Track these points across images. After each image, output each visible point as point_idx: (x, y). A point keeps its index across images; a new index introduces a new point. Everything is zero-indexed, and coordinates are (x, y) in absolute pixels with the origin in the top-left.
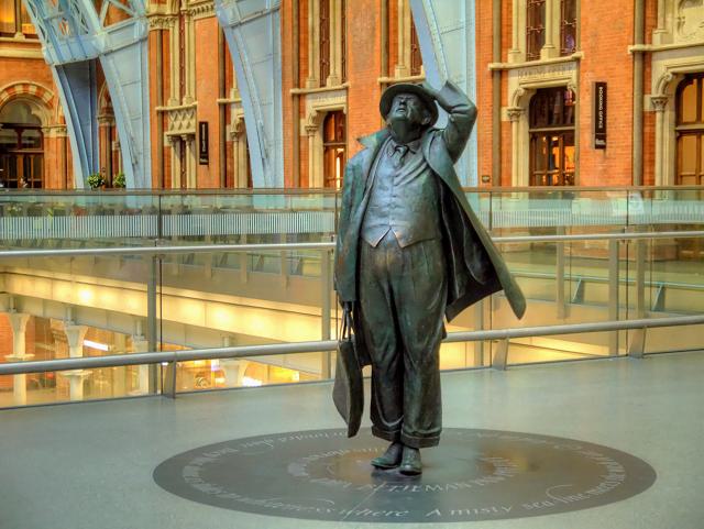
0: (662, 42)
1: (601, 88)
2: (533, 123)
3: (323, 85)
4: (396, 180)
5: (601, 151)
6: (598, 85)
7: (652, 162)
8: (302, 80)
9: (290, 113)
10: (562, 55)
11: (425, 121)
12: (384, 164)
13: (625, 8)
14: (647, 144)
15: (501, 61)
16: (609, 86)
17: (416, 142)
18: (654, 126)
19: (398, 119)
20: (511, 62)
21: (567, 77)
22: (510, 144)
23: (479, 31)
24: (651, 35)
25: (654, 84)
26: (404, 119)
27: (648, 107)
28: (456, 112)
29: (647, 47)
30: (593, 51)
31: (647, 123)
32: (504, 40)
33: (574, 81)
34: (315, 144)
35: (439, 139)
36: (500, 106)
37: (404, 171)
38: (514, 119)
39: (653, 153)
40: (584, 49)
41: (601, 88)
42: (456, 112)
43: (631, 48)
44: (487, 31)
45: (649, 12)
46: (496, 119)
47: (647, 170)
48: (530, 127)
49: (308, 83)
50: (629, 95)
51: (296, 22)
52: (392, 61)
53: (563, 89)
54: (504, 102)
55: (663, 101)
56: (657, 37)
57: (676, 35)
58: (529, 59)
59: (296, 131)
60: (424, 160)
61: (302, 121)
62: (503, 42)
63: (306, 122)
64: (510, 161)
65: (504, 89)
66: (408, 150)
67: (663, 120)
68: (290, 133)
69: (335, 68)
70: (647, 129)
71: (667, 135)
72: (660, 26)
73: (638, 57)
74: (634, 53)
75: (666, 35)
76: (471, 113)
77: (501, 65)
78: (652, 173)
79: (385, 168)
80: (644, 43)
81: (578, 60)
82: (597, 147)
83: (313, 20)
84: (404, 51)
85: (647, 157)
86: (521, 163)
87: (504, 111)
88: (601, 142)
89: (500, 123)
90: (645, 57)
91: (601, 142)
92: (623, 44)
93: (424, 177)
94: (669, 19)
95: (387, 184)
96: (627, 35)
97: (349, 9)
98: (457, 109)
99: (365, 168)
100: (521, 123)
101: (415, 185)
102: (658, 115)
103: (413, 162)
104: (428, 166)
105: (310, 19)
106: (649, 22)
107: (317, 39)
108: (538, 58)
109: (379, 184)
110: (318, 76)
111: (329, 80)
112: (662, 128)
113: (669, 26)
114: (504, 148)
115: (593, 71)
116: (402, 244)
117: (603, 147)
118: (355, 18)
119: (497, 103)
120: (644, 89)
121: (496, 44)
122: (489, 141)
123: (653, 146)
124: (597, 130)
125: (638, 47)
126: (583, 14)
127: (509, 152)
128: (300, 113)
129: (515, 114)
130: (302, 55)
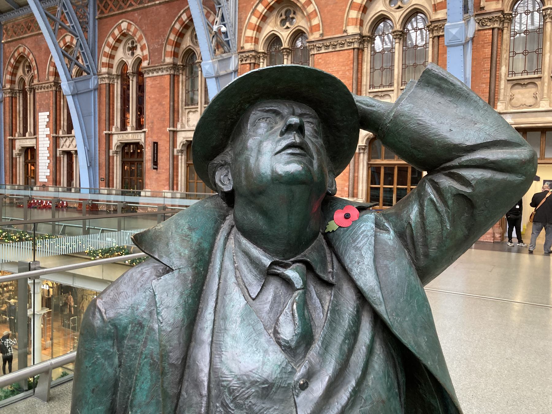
0: (181, 127)
1: (155, 144)
2: (123, 157)
3: (24, 135)
5: (155, 170)
6: (154, 143)
7: (177, 176)
8: (14, 133)
9: (8, 147)
10: (137, 129)
13: (166, 112)
14: (175, 168)
15: (109, 130)
16: (159, 143)
18: (178, 161)
20: (114, 131)
21: (140, 137)
22: (113, 166)
23: (100, 117)
24: (176, 124)
25: (178, 144)
27: (175, 153)
29: (175, 129)
30: (152, 129)
31: (175, 160)
32: (111, 122)
33: (143, 140)
34: (21, 161)
35: (389, 237)
36: (109, 149)
38: (115, 155)
39: (177, 172)
40: (148, 128)
41: (155, 144)
43: (168, 129)
44: (103, 117)
45: (176, 115)
46: (107, 154)
47: (175, 179)
48: (122, 158)
49: (17, 135)
50: (168, 148)
51: (10, 108)
52: (58, 127)
53: (137, 145)
54: (111, 147)
55: (181, 151)
56: (179, 127)
57: (186, 126)
58: (121, 130)
59: (11, 155)
61: (14, 151)
62: (110, 123)
63: (16, 152)
64: (113, 173)
65: (111, 142)
67: (181, 159)
68: (8, 156)
69: (30, 129)
70: (175, 163)
71: (183, 165)
72: (180, 121)
73: (171, 133)
74: (170, 131)
75: (183, 125)
77: (110, 132)
78: (177, 180)
80: (174, 127)
81: (144, 132)
82: (154, 169)
83: (19, 107)
84: (64, 123)
85: (175, 174)
86: (118, 173)
87: (111, 151)
88: (155, 167)
89: (109, 156)
90: (175, 132)
91: (155, 167)
92: (166, 127)
94: (184, 119)
96: (167, 123)
97: (37, 104)
100: (118, 157)
102: (180, 157)
105: (18, 107)
106: (176, 119)
107: (21, 116)
108: (126, 129)
110: (22, 132)
111: (27, 134)
112: (181, 162)
113: (184, 121)
114: (111, 167)
115: (152, 137)
117: (156, 169)
118: (40, 108)
119: (107, 148)
120: (174, 146)
121: (107, 123)
122: (104, 163)
123: (177, 169)
124: (154, 161)
125: (172, 129)
126: (147, 114)
127: (113, 169)
128: (13, 147)
129: (116, 152)
130: (14, 122)
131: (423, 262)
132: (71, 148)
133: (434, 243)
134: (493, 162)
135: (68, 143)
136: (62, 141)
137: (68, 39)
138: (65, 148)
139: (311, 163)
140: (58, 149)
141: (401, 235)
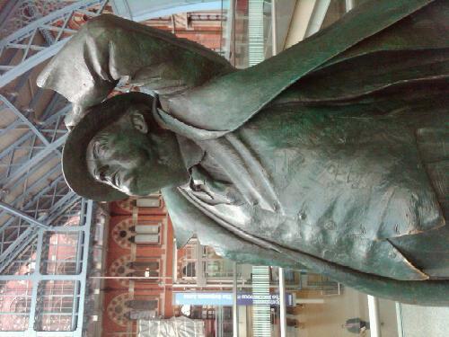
4: (264, 205)
11: (140, 123)
12: (227, 216)
17: (184, 150)
19: (133, 188)
26: (135, 176)
28: (106, 69)
35: (175, 103)
37: (246, 184)
42: (106, 69)
60: (222, 140)
66: (200, 168)
76: (101, 31)
79: (237, 216)
93: (261, 144)
95: (272, 223)
98: (98, 69)
99: (235, 244)
101: (279, 169)
103: (223, 160)
104: (237, 133)
109: (268, 235)
116: (431, 216)
131: (191, 85)
132: (185, 17)
133: (174, 82)
134: (102, 67)
135: (180, 20)
136: (179, 26)
137: (77, 19)
138: (185, 22)
139: (124, 170)
140: (187, 29)
141: (171, 96)
